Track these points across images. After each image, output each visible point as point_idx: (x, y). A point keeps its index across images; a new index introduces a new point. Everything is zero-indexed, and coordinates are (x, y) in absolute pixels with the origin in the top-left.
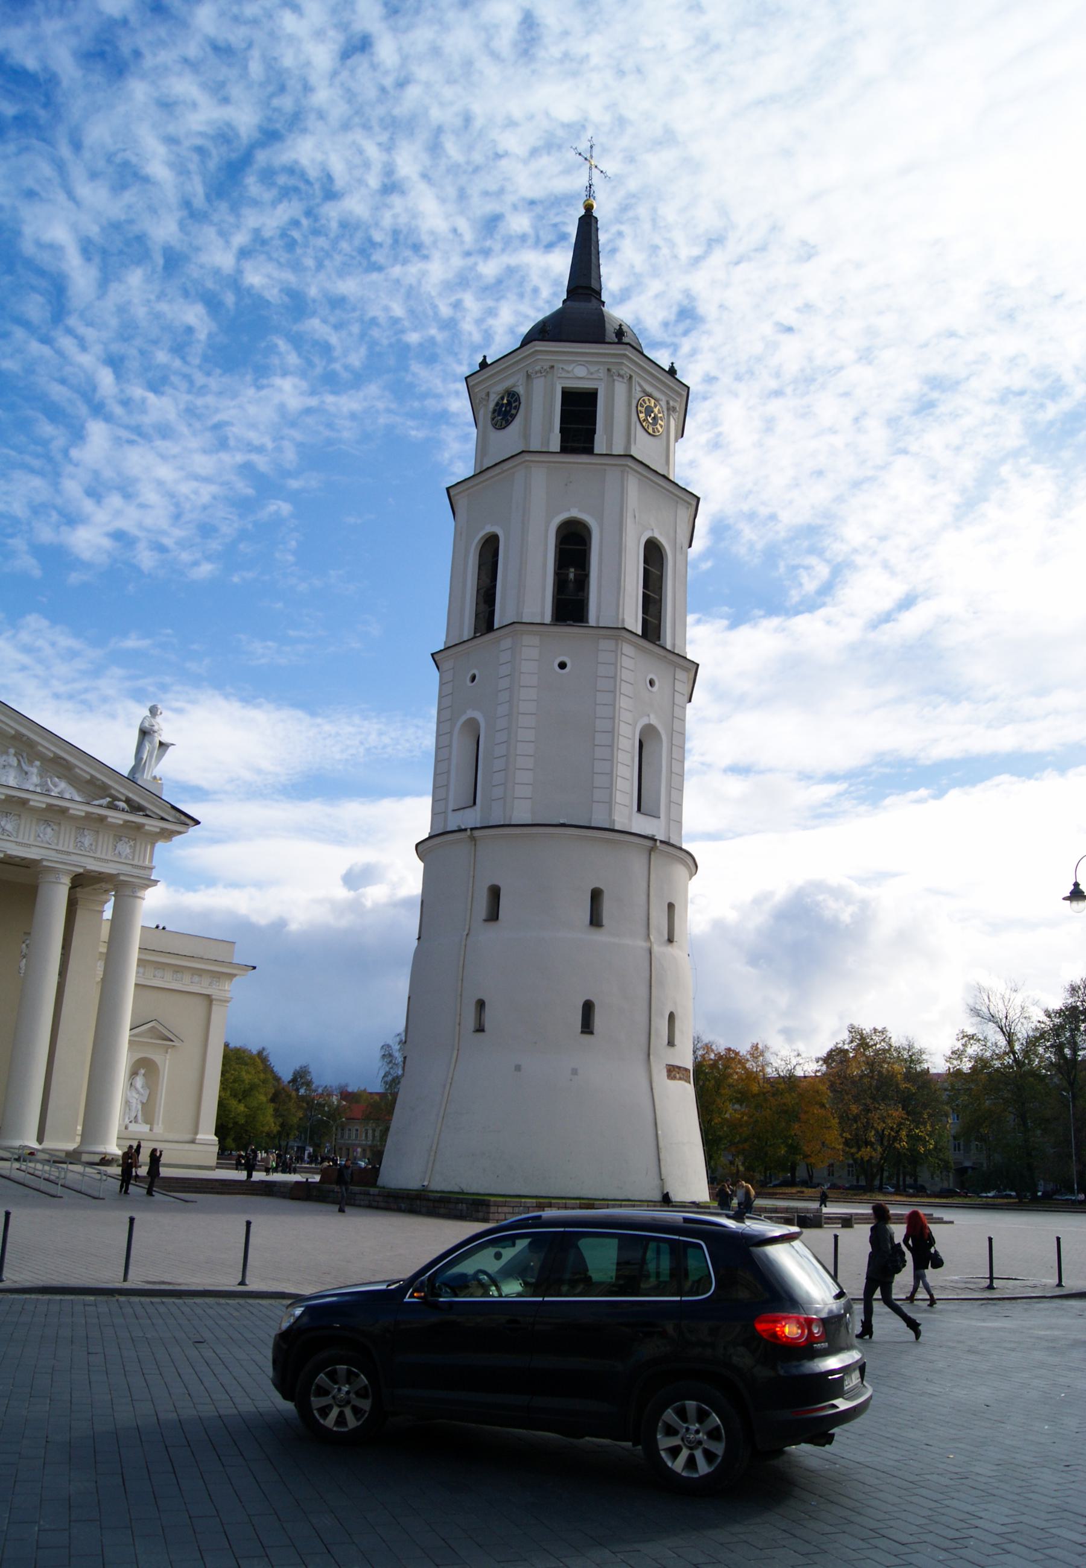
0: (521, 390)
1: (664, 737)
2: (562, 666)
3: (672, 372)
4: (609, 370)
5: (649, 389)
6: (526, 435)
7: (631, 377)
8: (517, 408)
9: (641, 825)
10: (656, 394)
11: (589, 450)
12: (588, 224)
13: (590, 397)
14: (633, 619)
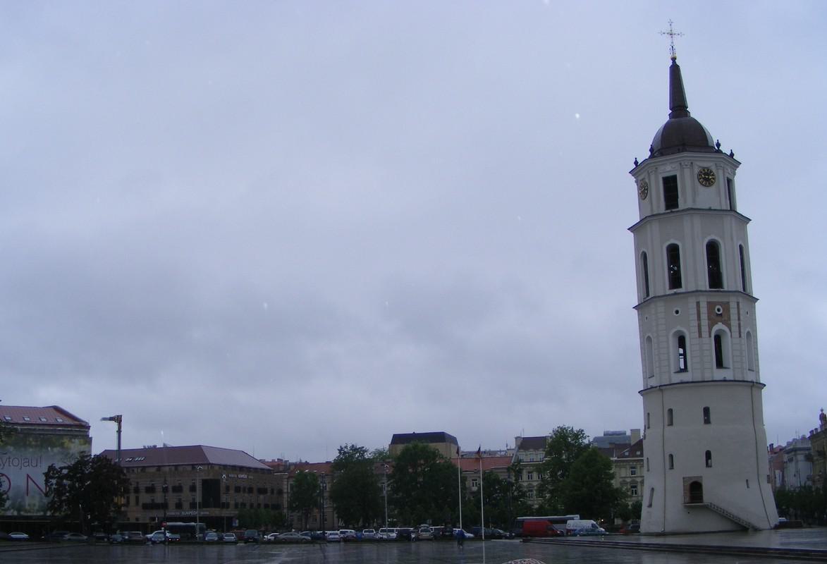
0: (647, 181)
2: (677, 312)
3: (718, 145)
4: (680, 164)
7: (692, 163)
8: (647, 189)
9: (720, 374)
11: (676, 206)
12: (675, 71)
13: (674, 178)
14: (704, 283)
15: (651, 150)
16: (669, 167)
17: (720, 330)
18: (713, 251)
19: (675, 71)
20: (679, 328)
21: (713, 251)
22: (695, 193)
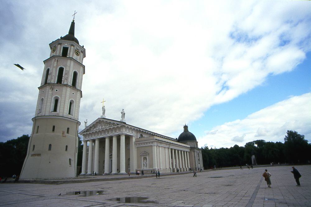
1: (75, 102)
2: (57, 90)
3: (83, 47)
5: (78, 48)
6: (56, 53)
10: (79, 49)
12: (73, 24)
15: (61, 37)
16: (66, 44)
17: (72, 100)
18: (75, 74)
19: (73, 24)
20: (57, 96)
21: (75, 74)
22: (73, 55)
